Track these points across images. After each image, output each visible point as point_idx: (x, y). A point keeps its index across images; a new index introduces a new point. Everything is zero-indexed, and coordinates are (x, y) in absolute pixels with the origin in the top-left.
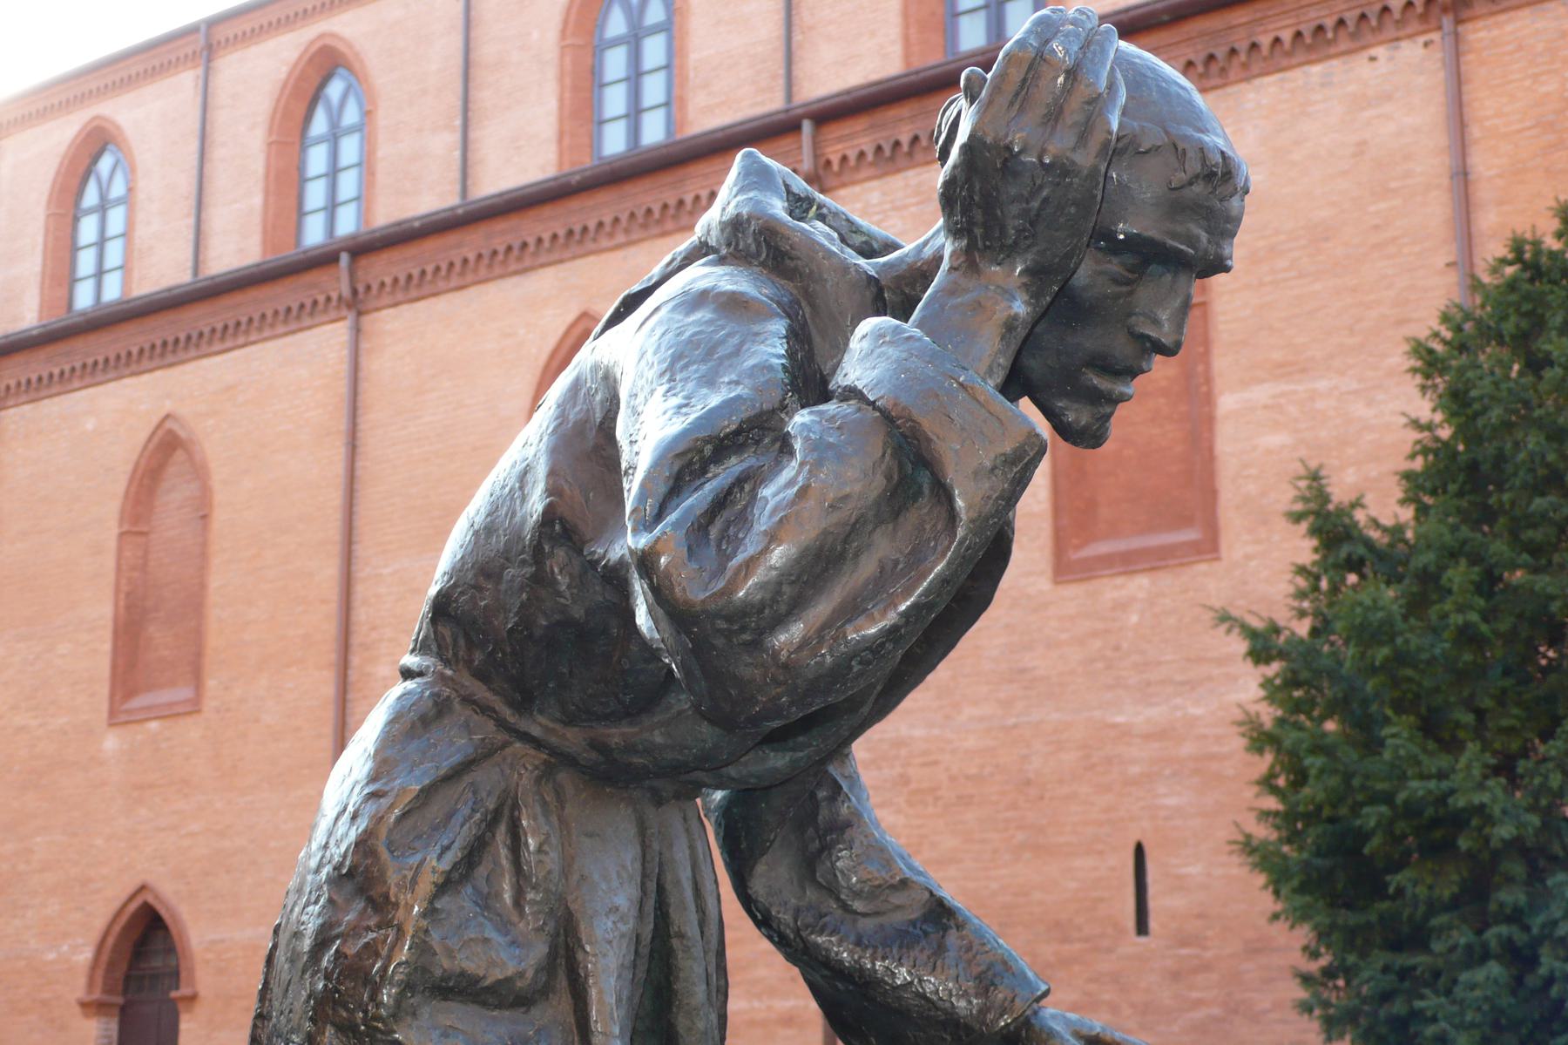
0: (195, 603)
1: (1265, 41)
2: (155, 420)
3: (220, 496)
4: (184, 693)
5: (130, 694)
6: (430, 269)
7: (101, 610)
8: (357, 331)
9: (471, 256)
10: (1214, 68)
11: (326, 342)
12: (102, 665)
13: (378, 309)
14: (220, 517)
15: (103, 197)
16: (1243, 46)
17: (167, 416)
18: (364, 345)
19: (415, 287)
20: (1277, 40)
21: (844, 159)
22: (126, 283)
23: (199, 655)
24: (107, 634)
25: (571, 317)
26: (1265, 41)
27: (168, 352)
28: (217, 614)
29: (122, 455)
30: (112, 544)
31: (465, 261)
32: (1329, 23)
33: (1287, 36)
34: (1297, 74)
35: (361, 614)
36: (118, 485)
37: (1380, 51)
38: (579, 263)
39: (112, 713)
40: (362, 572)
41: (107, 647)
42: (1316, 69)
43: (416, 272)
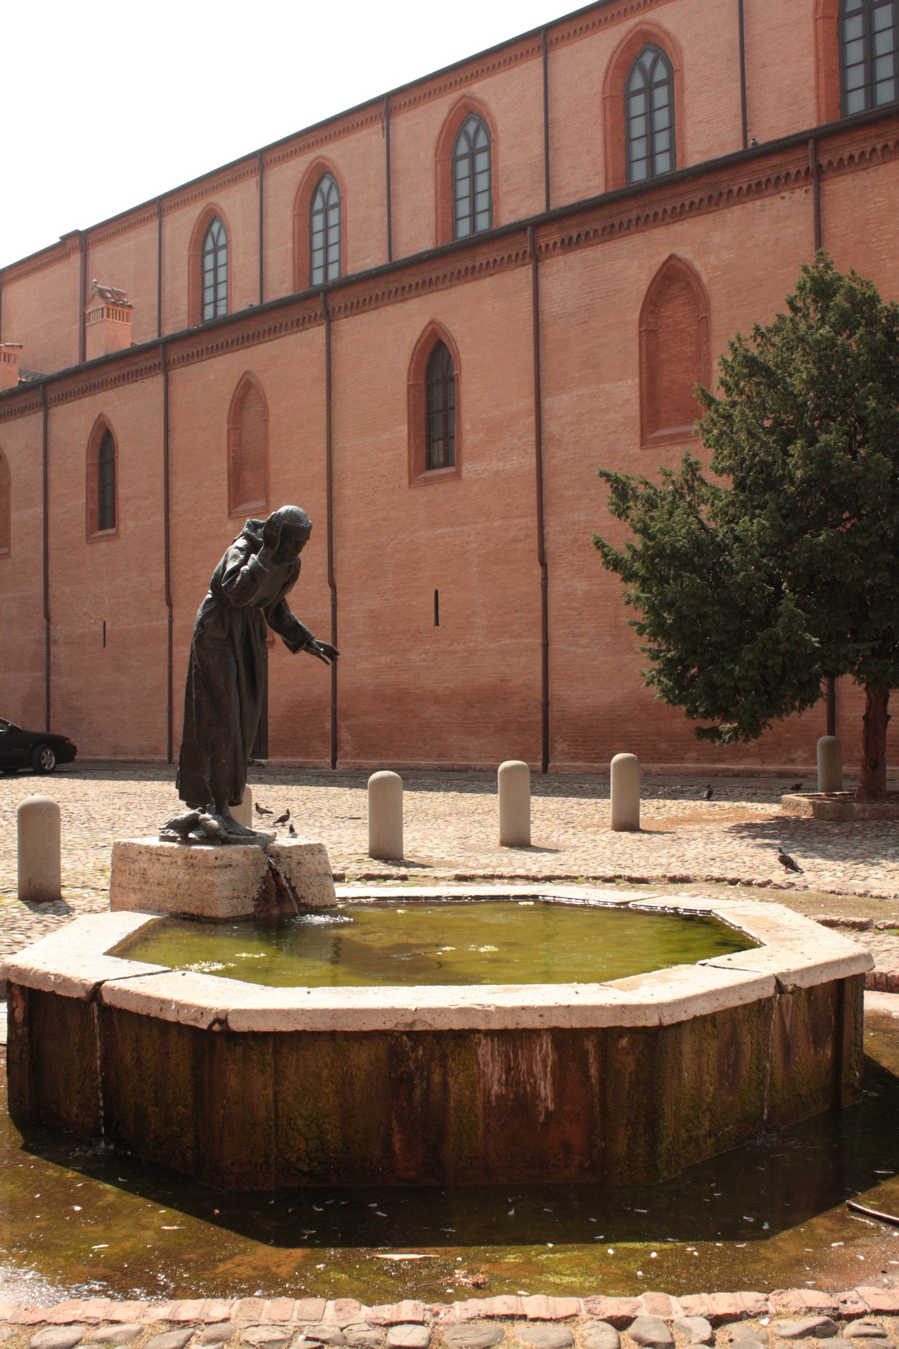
0: (263, 463)
1: (735, 189)
2: (241, 375)
3: (272, 410)
4: (261, 503)
5: (238, 504)
6: (361, 300)
7: (222, 466)
8: (329, 331)
9: (380, 293)
10: (713, 202)
12: (224, 490)
13: (338, 319)
14: (272, 420)
15: (215, 244)
16: (726, 191)
17: (246, 373)
18: (333, 337)
19: (355, 308)
20: (740, 189)
21: (547, 245)
22: (228, 306)
23: (267, 485)
24: (226, 477)
25: (426, 323)
26: (735, 189)
27: (245, 342)
28: (273, 466)
29: (227, 391)
30: (225, 434)
31: (377, 296)
32: (764, 180)
33: (745, 186)
34: (749, 205)
35: (337, 466)
36: (226, 406)
37: (786, 194)
38: (430, 296)
39: (230, 514)
40: (336, 446)
41: (226, 482)
42: (758, 203)
43: (355, 302)
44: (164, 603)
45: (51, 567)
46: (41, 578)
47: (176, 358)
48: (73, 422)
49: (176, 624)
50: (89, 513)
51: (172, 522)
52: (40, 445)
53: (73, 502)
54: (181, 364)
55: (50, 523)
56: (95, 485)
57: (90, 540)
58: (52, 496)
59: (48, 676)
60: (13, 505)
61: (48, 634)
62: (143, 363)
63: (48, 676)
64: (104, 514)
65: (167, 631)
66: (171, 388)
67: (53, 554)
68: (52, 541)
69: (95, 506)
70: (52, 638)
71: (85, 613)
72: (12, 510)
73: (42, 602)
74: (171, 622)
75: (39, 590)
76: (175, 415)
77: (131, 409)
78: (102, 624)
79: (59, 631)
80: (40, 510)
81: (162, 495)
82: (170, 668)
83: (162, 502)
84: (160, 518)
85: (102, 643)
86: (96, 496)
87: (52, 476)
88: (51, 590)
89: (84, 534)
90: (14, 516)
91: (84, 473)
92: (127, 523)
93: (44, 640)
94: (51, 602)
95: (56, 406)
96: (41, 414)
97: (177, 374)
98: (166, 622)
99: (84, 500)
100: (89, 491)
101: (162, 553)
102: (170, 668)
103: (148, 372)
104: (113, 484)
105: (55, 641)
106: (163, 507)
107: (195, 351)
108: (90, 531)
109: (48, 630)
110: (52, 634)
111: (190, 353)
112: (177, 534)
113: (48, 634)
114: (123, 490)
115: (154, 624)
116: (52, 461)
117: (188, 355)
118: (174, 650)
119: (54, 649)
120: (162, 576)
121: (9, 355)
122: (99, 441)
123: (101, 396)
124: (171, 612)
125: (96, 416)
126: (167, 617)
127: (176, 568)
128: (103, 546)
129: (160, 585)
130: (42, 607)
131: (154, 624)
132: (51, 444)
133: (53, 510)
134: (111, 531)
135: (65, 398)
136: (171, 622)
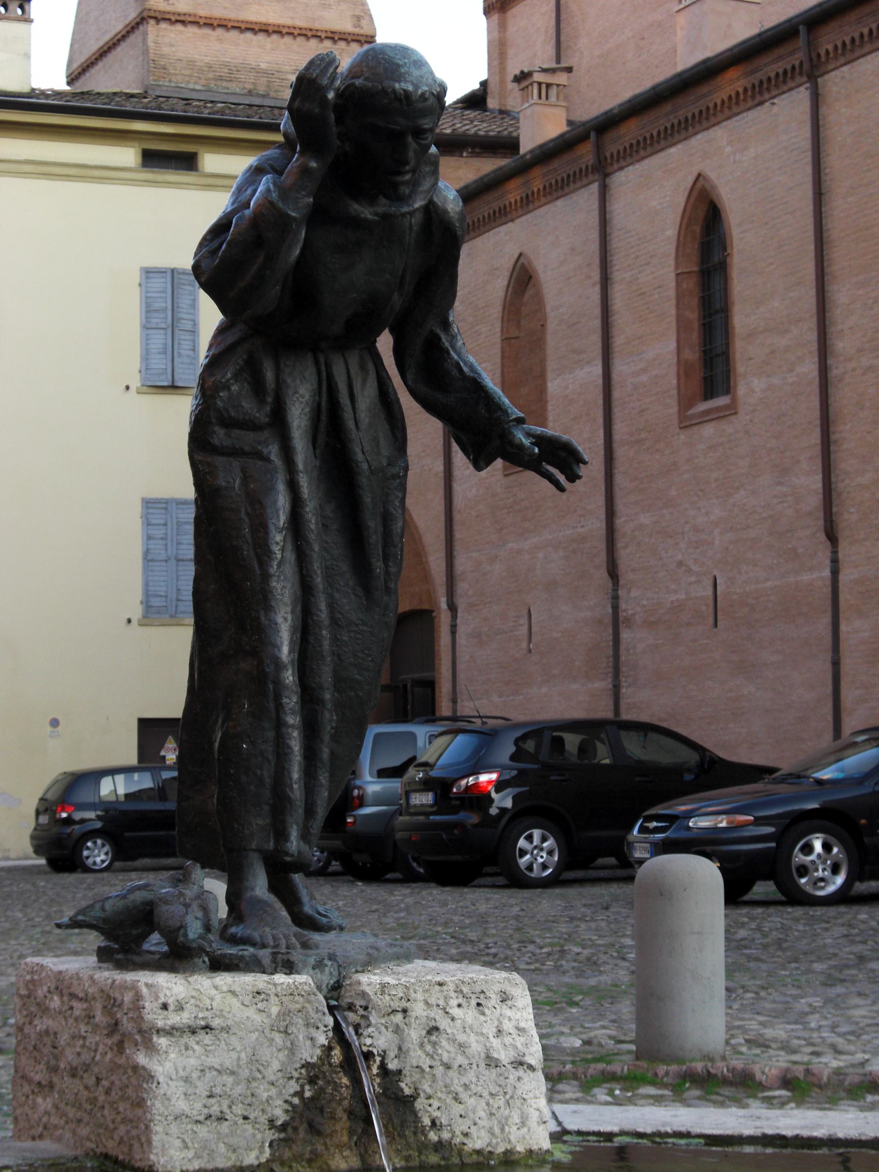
11: (790, 108)
44: (822, 537)
45: (620, 480)
46: (601, 500)
47: (830, 47)
48: (651, 195)
49: (845, 577)
50: (684, 369)
51: (834, 373)
52: (594, 246)
53: (654, 351)
54: (842, 60)
55: (616, 394)
56: (693, 315)
57: (686, 422)
58: (618, 341)
59: (616, 688)
60: (551, 365)
61: (616, 608)
62: (771, 65)
63: (616, 688)
64: (711, 369)
65: (828, 590)
66: (823, 110)
67: (620, 452)
68: (620, 429)
69: (693, 355)
70: (622, 615)
71: (680, 564)
72: (550, 375)
73: (602, 546)
74: (835, 573)
75: (597, 524)
76: (834, 161)
77: (749, 158)
78: (710, 582)
79: (634, 600)
80: (597, 370)
81: (813, 323)
82: (836, 664)
83: (813, 336)
84: (810, 368)
85: (711, 620)
86: (695, 336)
87: (618, 302)
88: (619, 522)
89: (674, 410)
90: (553, 386)
91: (672, 293)
92: (751, 384)
93: (608, 620)
94: (619, 544)
95: (621, 168)
96: (595, 187)
97: (837, 81)
98: (827, 573)
99: (673, 345)
100: (682, 325)
101: (816, 437)
102: (836, 664)
103: (780, 83)
104: (725, 311)
105: (627, 620)
106: (814, 347)
107: (866, 31)
108: (685, 403)
109: (615, 598)
110: (623, 605)
111: (856, 36)
112: (844, 397)
113: (616, 608)
114: (743, 319)
115: (806, 577)
116: (618, 275)
117: (853, 40)
118: (843, 627)
119: (625, 635)
120: (816, 482)
121: (548, 86)
122: (698, 229)
123: (698, 141)
124: (835, 552)
125: (691, 180)
126: (828, 562)
127: (846, 463)
128: (708, 430)
129: (814, 501)
130: (603, 556)
131: (806, 577)
132: (617, 243)
133: (620, 368)
134: (721, 401)
135: (636, 151)
136: (835, 573)
